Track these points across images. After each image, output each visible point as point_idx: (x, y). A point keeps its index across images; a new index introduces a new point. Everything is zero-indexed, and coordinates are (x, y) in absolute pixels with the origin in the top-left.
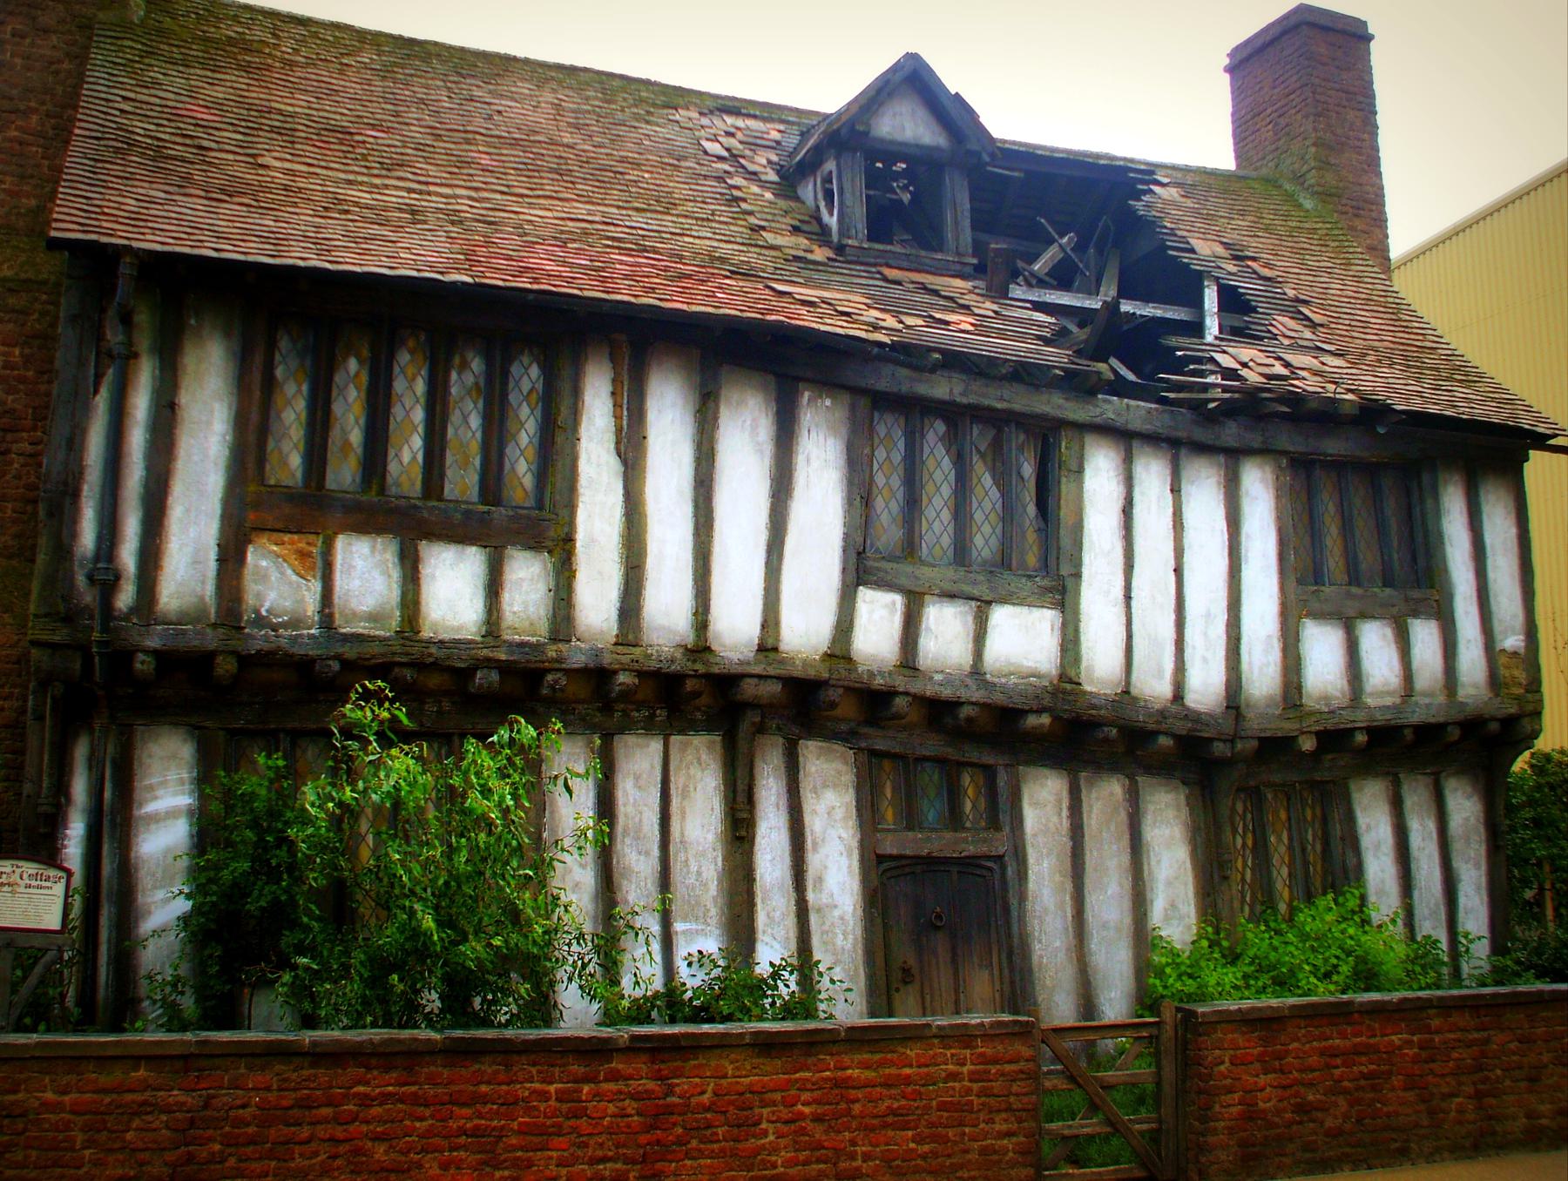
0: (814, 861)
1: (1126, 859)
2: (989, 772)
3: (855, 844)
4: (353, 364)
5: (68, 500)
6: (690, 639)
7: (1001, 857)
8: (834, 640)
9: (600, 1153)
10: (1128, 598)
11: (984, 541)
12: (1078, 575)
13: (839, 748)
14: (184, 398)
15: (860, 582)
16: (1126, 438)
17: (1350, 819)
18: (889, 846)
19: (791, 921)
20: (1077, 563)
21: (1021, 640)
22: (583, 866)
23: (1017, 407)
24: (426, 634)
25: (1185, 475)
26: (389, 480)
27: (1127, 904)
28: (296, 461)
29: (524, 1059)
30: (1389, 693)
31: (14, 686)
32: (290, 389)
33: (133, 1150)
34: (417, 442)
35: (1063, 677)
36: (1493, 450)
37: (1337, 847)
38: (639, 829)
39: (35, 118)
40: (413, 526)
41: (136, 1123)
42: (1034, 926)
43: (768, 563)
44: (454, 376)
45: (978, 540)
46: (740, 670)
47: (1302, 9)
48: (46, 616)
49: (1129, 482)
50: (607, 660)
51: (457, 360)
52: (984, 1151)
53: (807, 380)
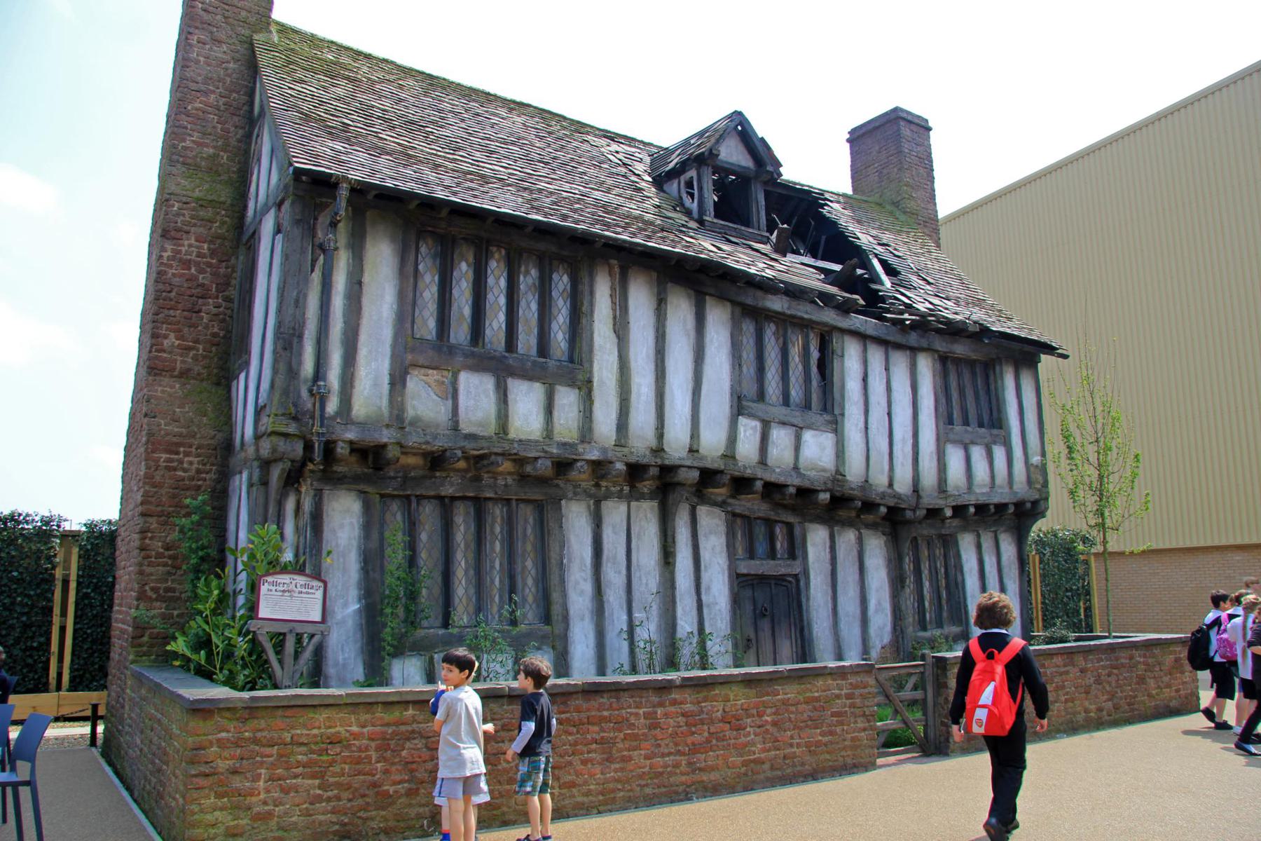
0: (705, 577)
1: (857, 577)
2: (790, 527)
3: (726, 567)
4: (464, 266)
5: (295, 340)
6: (653, 443)
7: (796, 576)
8: (727, 447)
9: (666, 751)
10: (866, 428)
11: (796, 393)
12: (843, 415)
13: (717, 510)
14: (366, 279)
19: (694, 613)
20: (842, 408)
21: (817, 449)
22: (585, 580)
23: (814, 318)
24: (512, 435)
26: (487, 340)
27: (858, 601)
28: (432, 323)
29: (626, 694)
31: (213, 465)
32: (428, 278)
33: (407, 763)
34: (502, 317)
35: (838, 472)
36: (1026, 353)
37: (952, 572)
38: (615, 557)
39: (213, 96)
40: (502, 368)
41: (408, 745)
42: (814, 614)
43: (693, 400)
44: (522, 278)
46: (678, 463)
47: (896, 110)
48: (283, 415)
49: (865, 363)
50: (610, 455)
51: (523, 269)
52: (853, 739)
53: (711, 295)
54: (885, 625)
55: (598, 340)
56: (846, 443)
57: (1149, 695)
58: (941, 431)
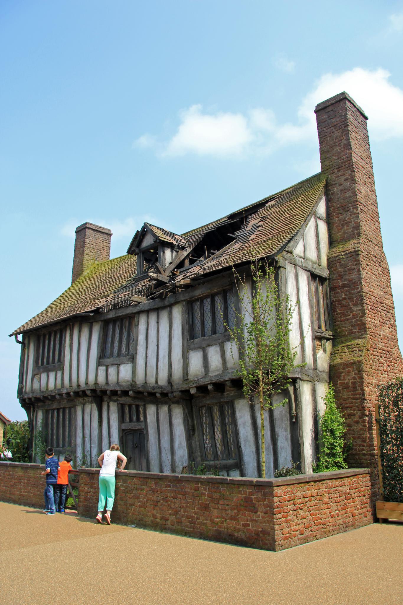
10: (146, 356)
15: (99, 365)
17: (233, 414)
23: (124, 314)
25: (160, 317)
30: (218, 370)
35: (133, 381)
54: (184, 456)
55: (66, 353)
56: (137, 367)
57: (212, 521)
58: (185, 345)
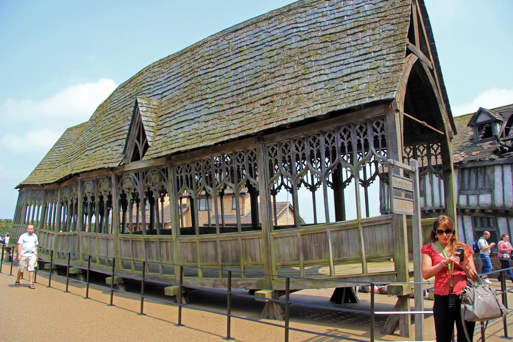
0: (466, 232)
10: (503, 190)
12: (494, 188)
16: (502, 165)
18: (477, 230)
21: (485, 199)
45: (479, 185)
